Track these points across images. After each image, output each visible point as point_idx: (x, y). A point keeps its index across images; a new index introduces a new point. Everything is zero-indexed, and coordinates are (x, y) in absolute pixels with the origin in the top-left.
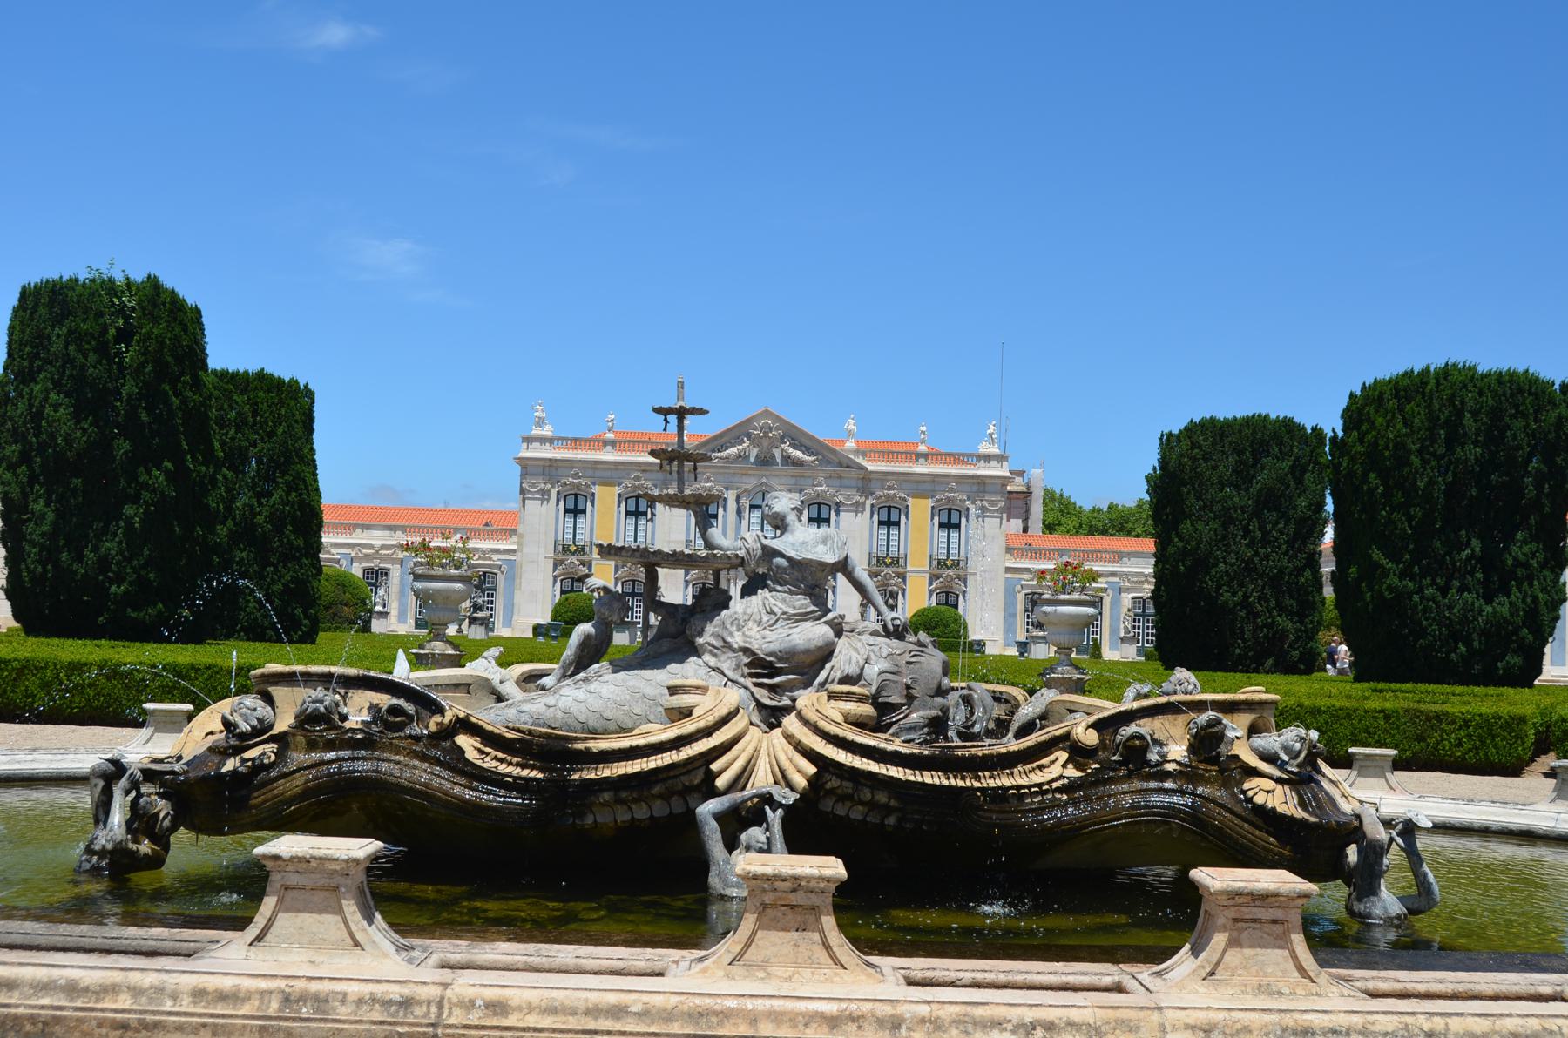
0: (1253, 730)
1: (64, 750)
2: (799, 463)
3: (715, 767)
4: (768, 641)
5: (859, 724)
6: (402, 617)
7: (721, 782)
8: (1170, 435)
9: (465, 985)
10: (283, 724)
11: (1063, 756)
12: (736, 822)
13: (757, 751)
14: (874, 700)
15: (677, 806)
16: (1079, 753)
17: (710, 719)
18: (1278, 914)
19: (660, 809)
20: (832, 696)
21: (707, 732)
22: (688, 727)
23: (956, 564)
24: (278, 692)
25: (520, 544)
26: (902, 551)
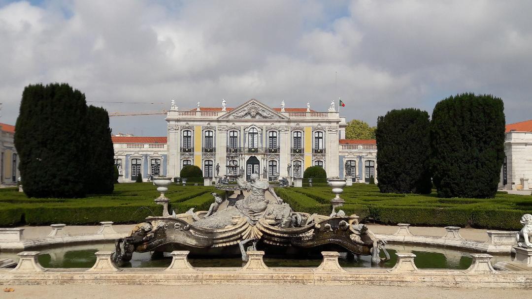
0: (353, 223)
1: (92, 234)
2: (265, 117)
3: (242, 234)
4: (254, 206)
5: (273, 225)
6: (127, 176)
7: (244, 238)
8: (382, 118)
9: (205, 273)
10: (155, 228)
11: (313, 230)
12: (247, 246)
13: (251, 231)
14: (276, 220)
15: (235, 243)
16: (317, 231)
17: (242, 225)
18: (334, 259)
19: (232, 243)
20: (266, 219)
21: (241, 227)
22: (237, 226)
23: (321, 151)
24: (153, 223)
25: (168, 149)
26: (302, 147)
